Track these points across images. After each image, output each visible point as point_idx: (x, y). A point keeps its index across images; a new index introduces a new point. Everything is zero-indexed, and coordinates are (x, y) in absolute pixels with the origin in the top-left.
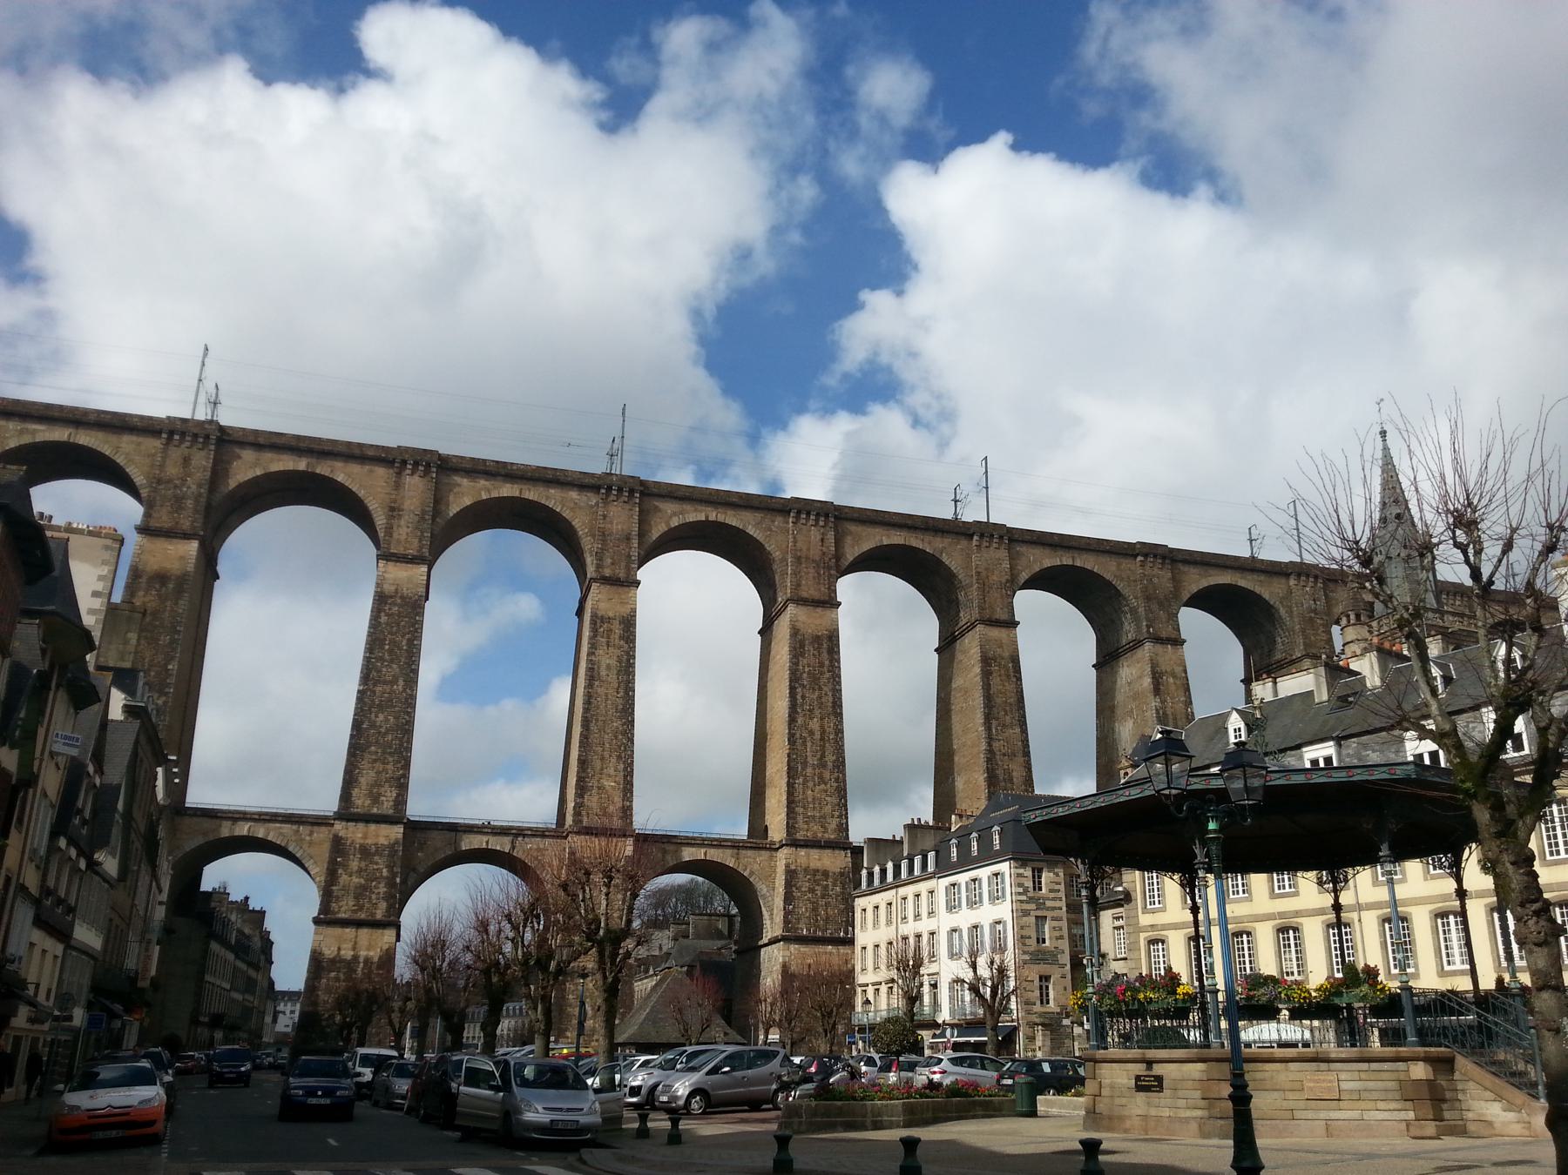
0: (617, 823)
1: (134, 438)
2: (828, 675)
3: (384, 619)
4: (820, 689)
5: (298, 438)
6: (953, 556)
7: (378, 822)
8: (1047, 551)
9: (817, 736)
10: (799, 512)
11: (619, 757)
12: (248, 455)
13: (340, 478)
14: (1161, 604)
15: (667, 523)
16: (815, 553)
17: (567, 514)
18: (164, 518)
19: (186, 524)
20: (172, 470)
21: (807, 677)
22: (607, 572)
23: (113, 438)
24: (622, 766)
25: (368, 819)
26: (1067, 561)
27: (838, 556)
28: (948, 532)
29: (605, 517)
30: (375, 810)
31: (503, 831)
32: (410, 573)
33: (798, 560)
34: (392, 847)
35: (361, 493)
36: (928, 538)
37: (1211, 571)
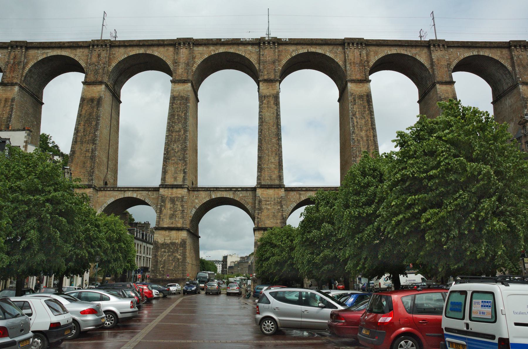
0: (277, 182)
1: (81, 50)
2: (367, 112)
3: (175, 106)
4: (364, 118)
5: (140, 41)
6: (422, 57)
7: (177, 188)
8: (466, 50)
9: (365, 139)
10: (349, 44)
11: (276, 154)
12: (122, 50)
13: (156, 54)
15: (291, 55)
16: (357, 60)
17: (247, 56)
18: (92, 78)
19: (100, 79)
20: (94, 60)
21: (355, 114)
22: (266, 77)
23: (74, 51)
24: (277, 158)
25: (173, 187)
26: (475, 53)
29: (263, 55)
30: (175, 183)
31: (230, 189)
32: (184, 87)
34: (183, 197)
35: (164, 59)
36: (409, 49)
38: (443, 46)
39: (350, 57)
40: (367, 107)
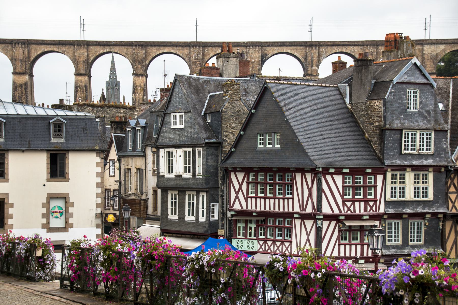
2: (24, 96)
8: (102, 47)
10: (15, 44)
14: (139, 63)
16: (21, 57)
27: (29, 57)
28: (67, 45)
33: (16, 60)
37: (161, 48)
38: (84, 45)
39: (16, 55)
40: (24, 92)
